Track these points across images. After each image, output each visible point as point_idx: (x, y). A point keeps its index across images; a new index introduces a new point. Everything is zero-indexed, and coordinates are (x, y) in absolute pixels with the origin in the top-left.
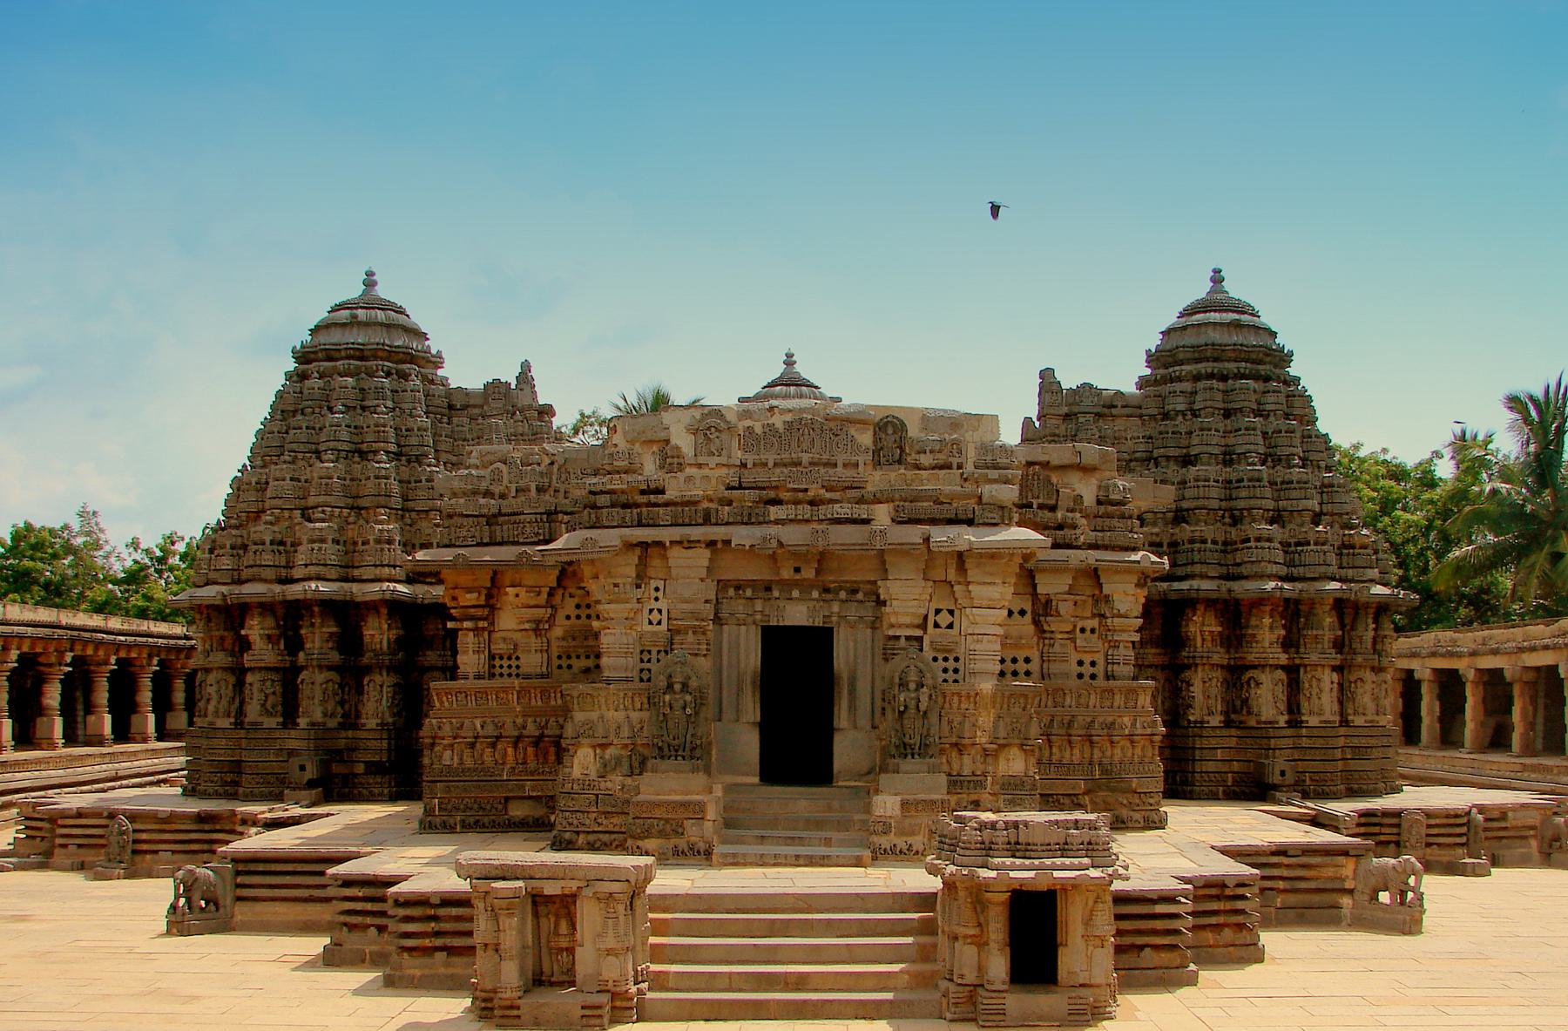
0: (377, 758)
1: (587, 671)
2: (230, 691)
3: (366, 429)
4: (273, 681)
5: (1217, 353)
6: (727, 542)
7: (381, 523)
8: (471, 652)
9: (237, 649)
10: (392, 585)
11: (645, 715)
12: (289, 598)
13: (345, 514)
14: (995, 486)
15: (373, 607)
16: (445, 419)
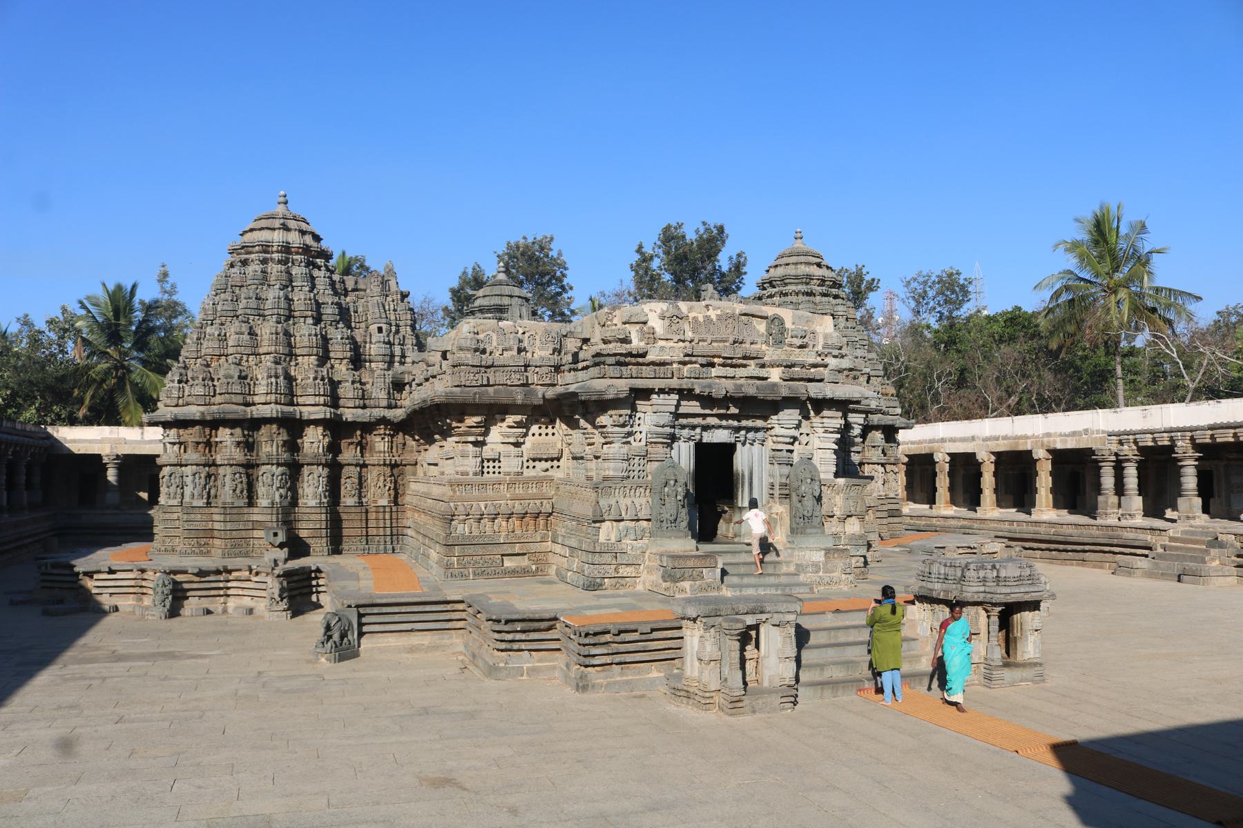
0: (318, 526)
1: (547, 470)
2: (203, 481)
3: (296, 302)
4: (240, 473)
5: (809, 278)
6: (691, 390)
7: (318, 366)
8: (471, 457)
9: (207, 451)
10: (332, 410)
11: (643, 500)
12: (255, 416)
13: (288, 359)
14: (838, 360)
15: (316, 423)
16: (342, 297)
